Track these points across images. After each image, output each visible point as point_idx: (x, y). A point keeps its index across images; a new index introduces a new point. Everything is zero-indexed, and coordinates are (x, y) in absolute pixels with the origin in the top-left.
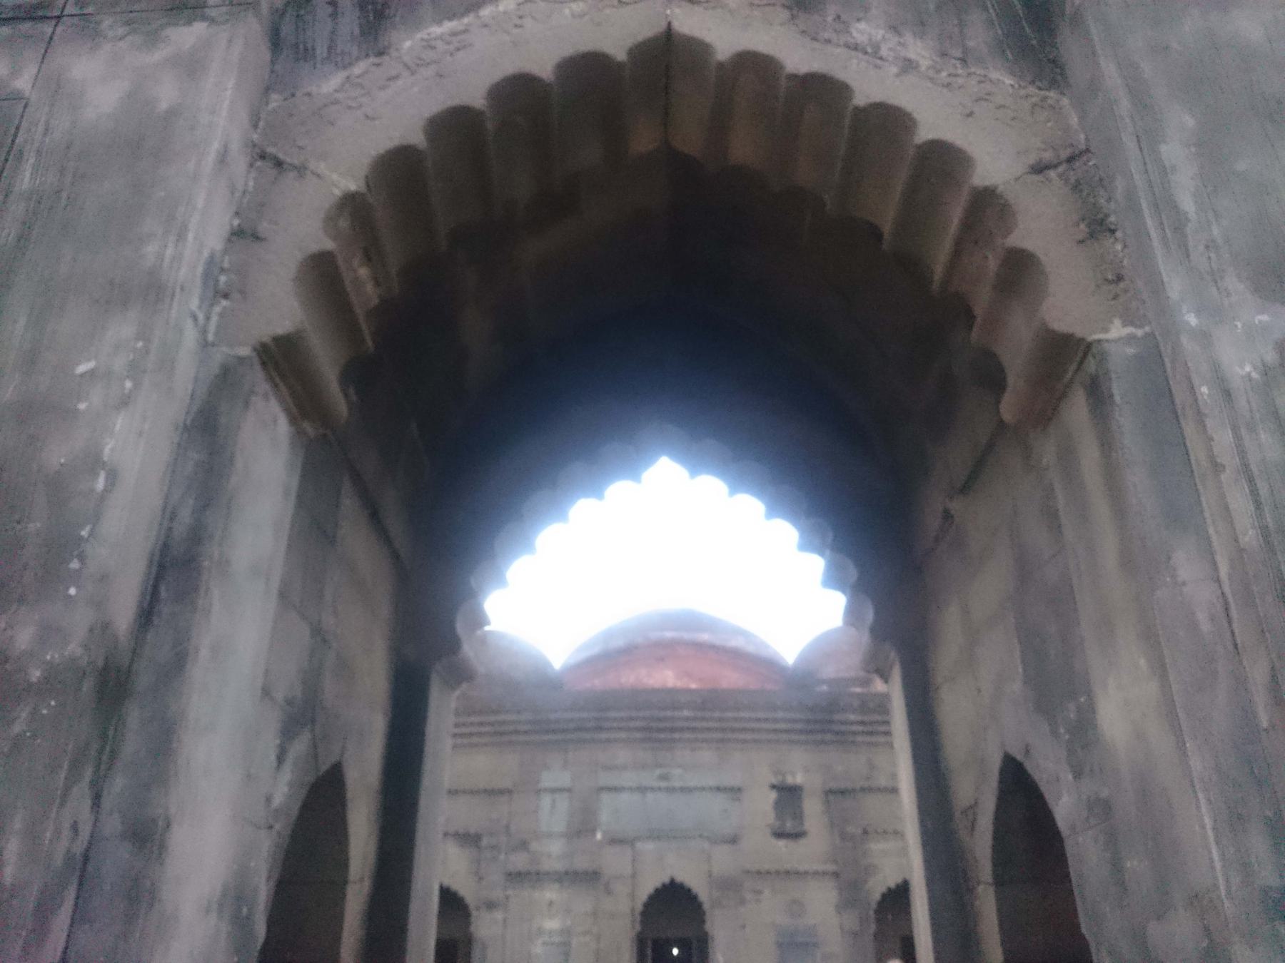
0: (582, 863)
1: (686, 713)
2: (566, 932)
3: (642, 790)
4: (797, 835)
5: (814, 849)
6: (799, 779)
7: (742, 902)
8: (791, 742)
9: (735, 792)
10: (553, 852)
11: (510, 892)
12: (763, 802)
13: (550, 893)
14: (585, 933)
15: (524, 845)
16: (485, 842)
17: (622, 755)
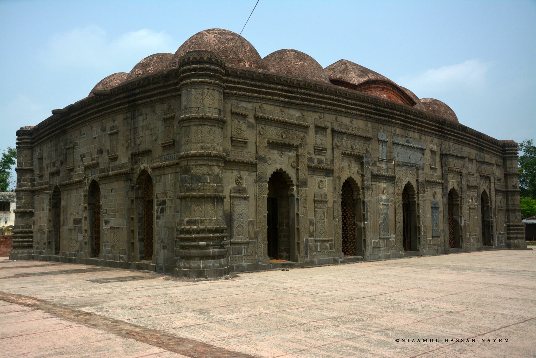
0: (391, 174)
1: (411, 117)
2: (388, 200)
3: (404, 146)
4: (433, 169)
5: (436, 176)
6: (435, 148)
7: (425, 192)
8: (435, 134)
9: (422, 150)
10: (383, 169)
11: (373, 183)
12: (428, 154)
13: (383, 185)
14: (392, 200)
15: (375, 164)
16: (365, 160)
17: (398, 131)
